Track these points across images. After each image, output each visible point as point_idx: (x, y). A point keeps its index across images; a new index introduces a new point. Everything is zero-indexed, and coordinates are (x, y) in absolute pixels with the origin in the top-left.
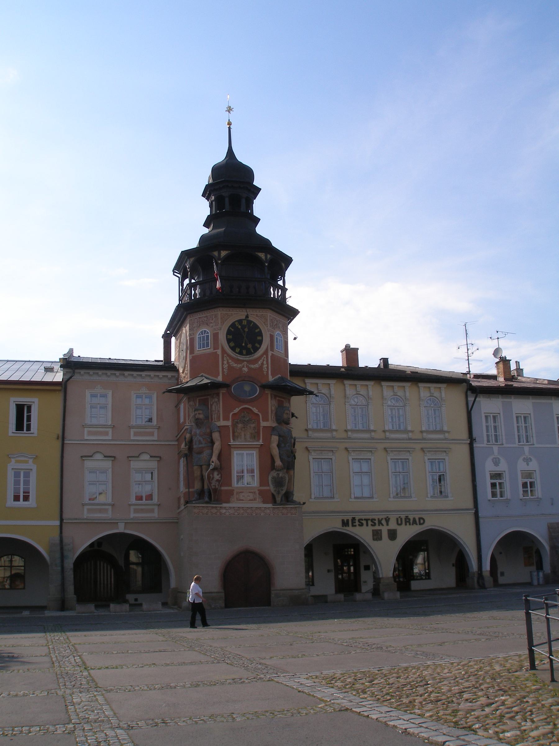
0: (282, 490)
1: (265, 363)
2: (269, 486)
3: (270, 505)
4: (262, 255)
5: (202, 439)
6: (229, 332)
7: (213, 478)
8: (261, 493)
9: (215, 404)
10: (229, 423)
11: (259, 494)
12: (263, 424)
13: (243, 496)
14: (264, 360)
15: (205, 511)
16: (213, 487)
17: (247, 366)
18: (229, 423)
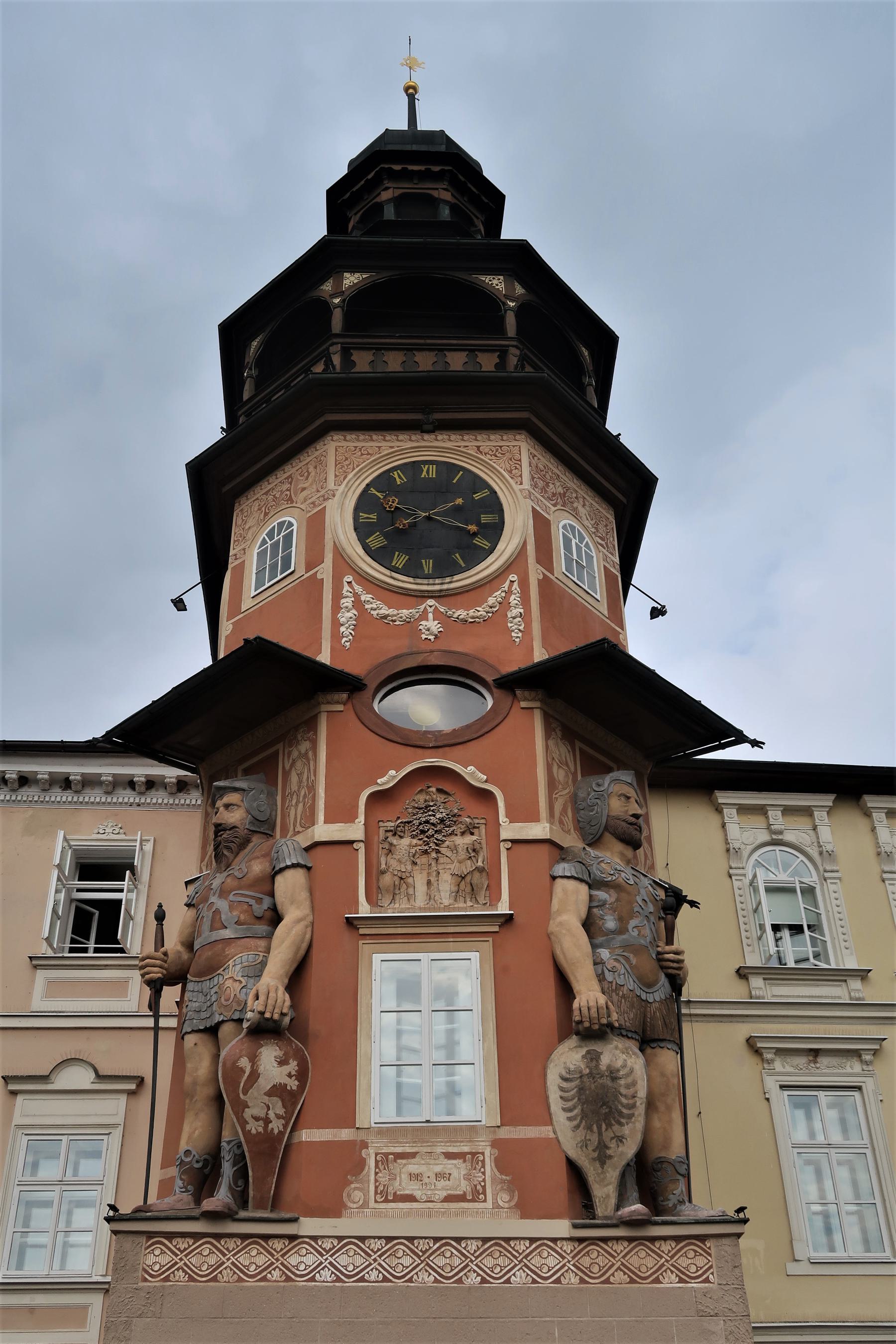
0: (620, 1139)
1: (514, 599)
2: (548, 1119)
3: (561, 1227)
4: (497, 283)
5: (222, 905)
6: (364, 502)
7: (254, 1076)
8: (508, 1156)
9: (299, 764)
10: (355, 831)
11: (500, 1164)
12: (509, 830)
13: (416, 1177)
14: (509, 592)
15: (205, 1257)
16: (254, 1127)
17: (437, 615)
18: (355, 831)
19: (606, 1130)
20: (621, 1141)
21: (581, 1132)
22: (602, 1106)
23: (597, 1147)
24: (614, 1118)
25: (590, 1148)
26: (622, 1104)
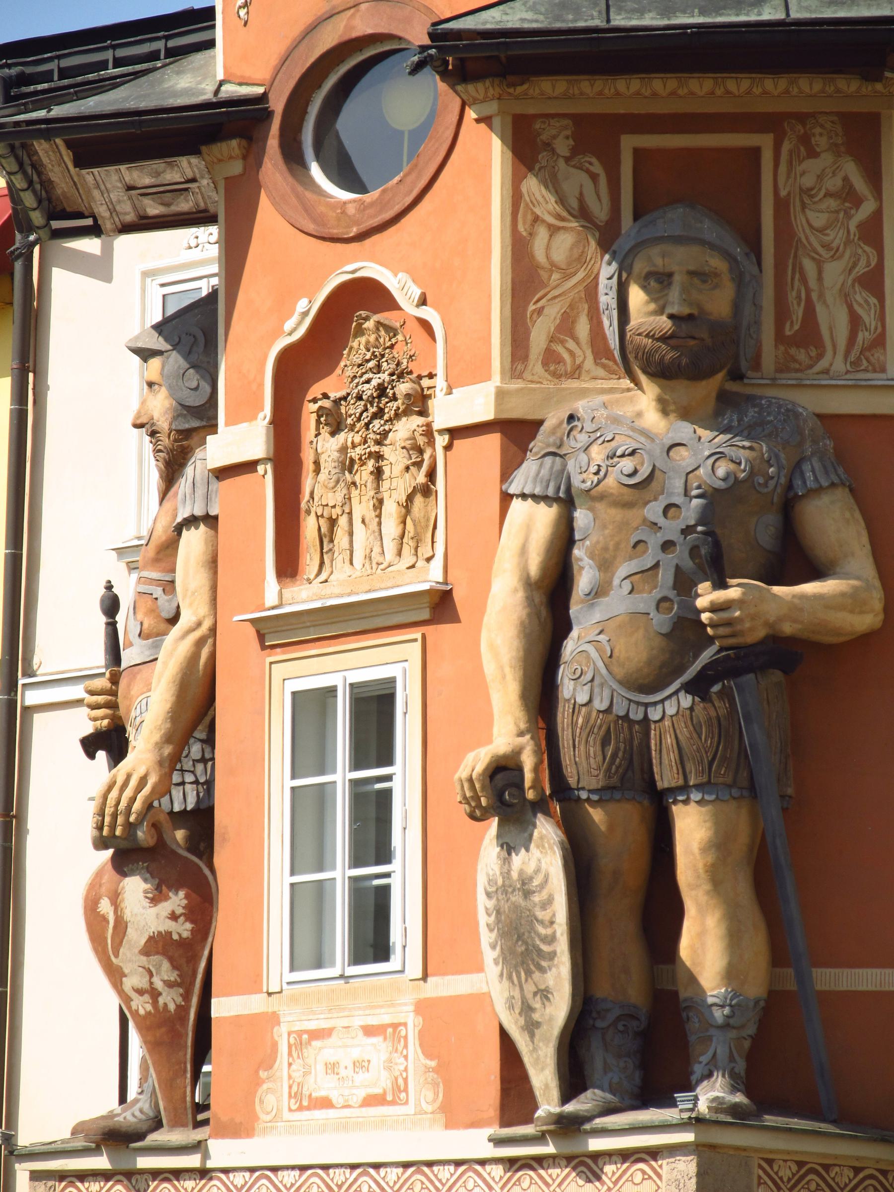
19: (526, 980)
20: (548, 999)
21: (506, 983)
22: (517, 941)
23: (522, 1010)
24: (533, 960)
25: (517, 1011)
26: (539, 935)
